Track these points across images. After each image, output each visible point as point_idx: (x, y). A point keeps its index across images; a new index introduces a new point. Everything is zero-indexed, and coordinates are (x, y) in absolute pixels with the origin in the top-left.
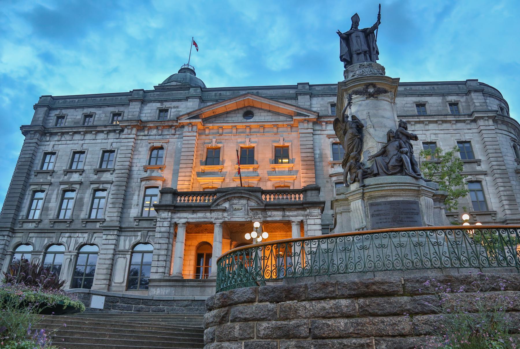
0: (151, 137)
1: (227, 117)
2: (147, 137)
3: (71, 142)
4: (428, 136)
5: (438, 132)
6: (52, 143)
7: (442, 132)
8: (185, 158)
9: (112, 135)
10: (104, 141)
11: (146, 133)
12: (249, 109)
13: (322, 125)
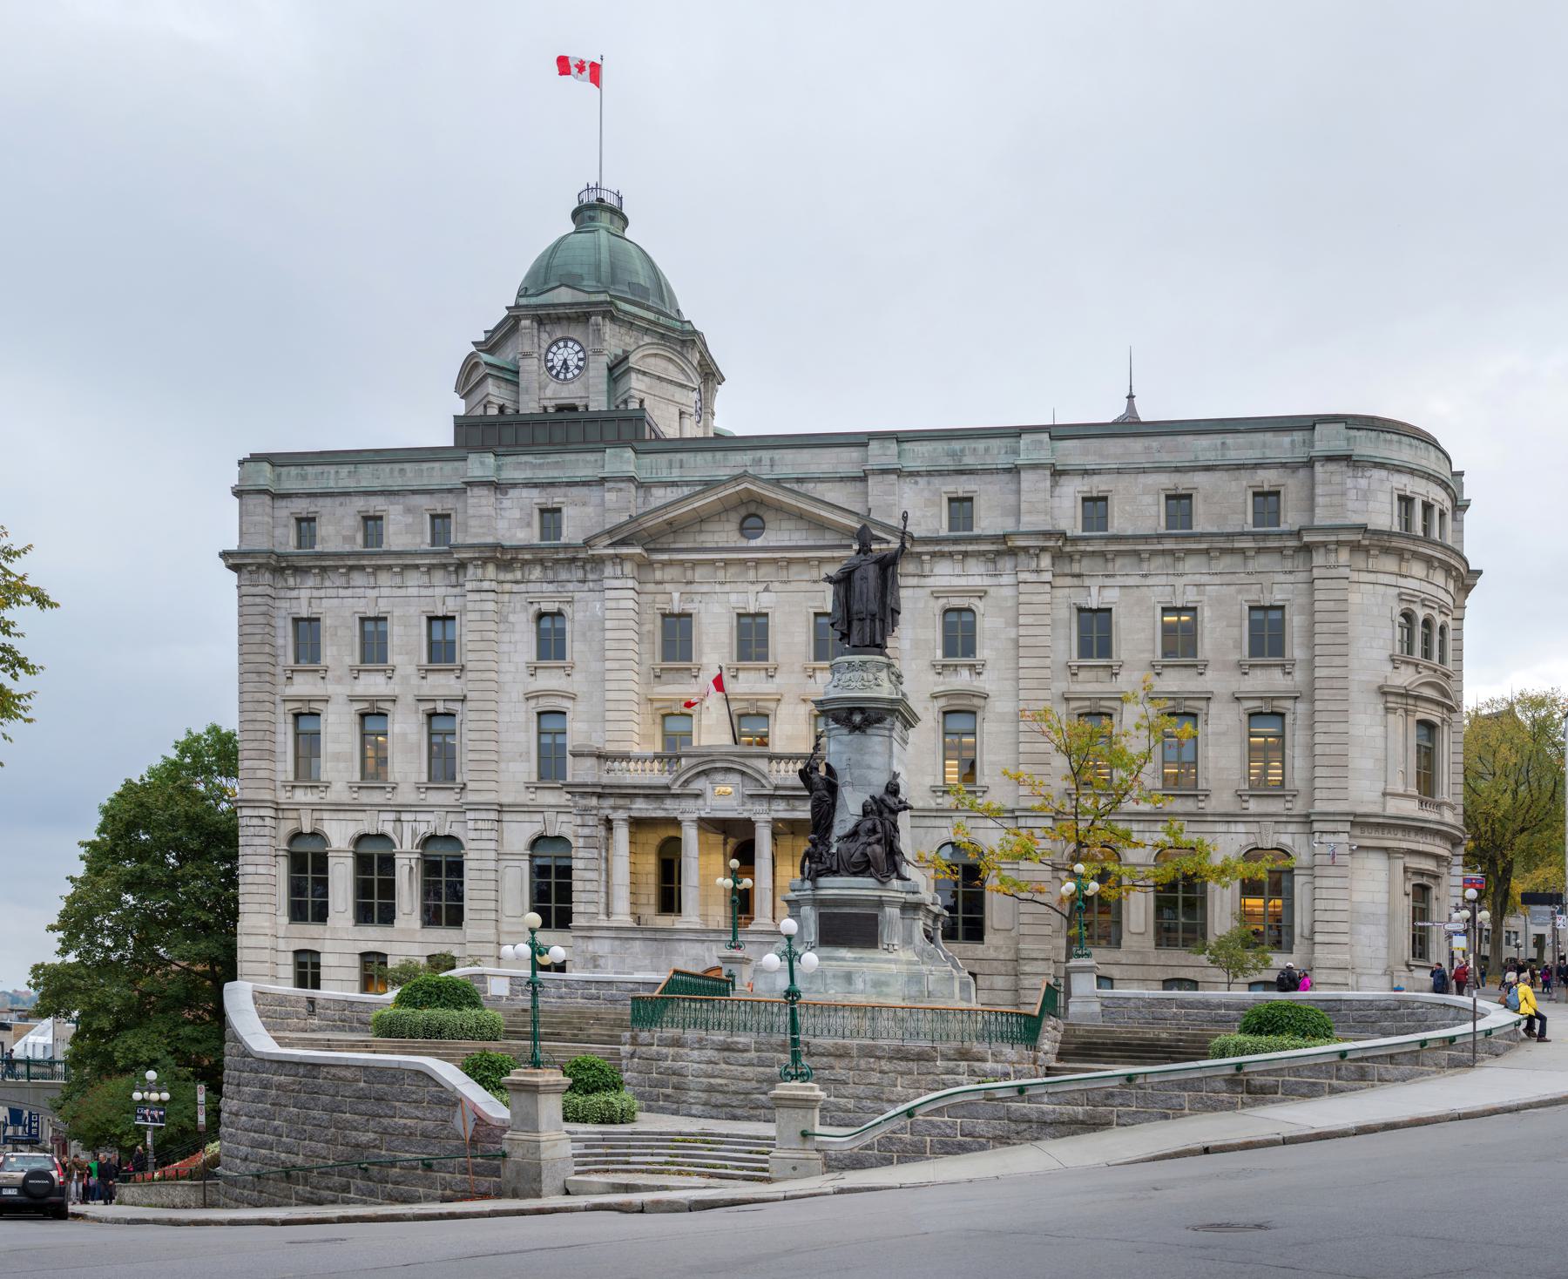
0: (531, 587)
1: (701, 532)
2: (522, 587)
3: (349, 592)
4: (1179, 591)
5: (1205, 579)
6: (304, 594)
7: (1217, 579)
8: (615, 645)
9: (438, 576)
10: (424, 592)
11: (518, 575)
12: (752, 509)
13: (922, 562)
